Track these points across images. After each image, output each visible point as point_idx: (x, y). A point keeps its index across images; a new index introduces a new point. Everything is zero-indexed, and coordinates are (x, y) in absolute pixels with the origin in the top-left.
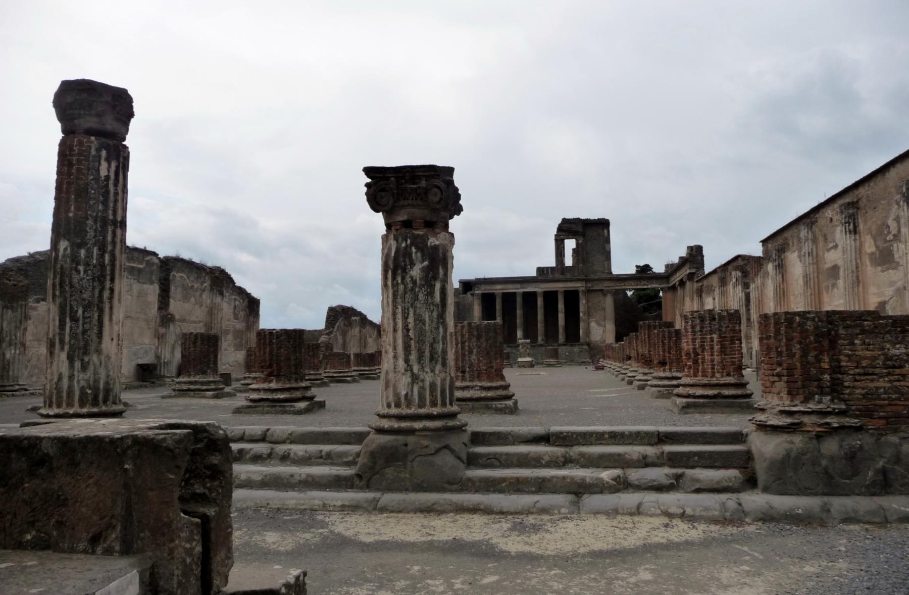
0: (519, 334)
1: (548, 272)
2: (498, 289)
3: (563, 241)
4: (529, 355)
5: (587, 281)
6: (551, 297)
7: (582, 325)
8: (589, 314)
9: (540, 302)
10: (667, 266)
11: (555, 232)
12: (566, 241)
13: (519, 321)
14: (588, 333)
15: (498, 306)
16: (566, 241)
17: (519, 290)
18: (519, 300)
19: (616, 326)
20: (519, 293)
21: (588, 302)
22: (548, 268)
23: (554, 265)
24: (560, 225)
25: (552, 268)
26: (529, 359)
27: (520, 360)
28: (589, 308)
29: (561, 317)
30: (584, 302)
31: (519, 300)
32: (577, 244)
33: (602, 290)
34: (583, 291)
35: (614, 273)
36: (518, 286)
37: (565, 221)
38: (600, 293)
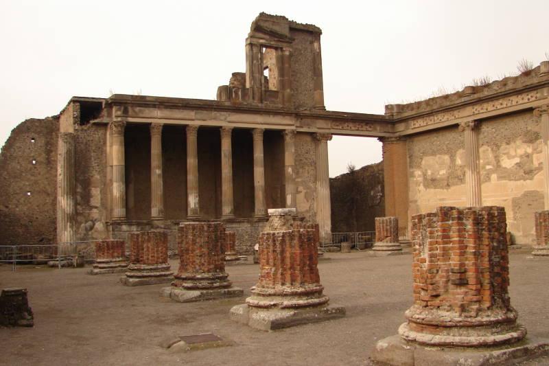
0: (193, 201)
2: (158, 118)
5: (298, 116)
6: (242, 138)
9: (226, 145)
10: (387, 107)
11: (247, 30)
13: (192, 177)
17: (194, 121)
18: (192, 140)
29: (259, 172)
31: (192, 140)
33: (312, 134)
34: (293, 132)
36: (192, 114)
37: (263, 15)
38: (308, 139)
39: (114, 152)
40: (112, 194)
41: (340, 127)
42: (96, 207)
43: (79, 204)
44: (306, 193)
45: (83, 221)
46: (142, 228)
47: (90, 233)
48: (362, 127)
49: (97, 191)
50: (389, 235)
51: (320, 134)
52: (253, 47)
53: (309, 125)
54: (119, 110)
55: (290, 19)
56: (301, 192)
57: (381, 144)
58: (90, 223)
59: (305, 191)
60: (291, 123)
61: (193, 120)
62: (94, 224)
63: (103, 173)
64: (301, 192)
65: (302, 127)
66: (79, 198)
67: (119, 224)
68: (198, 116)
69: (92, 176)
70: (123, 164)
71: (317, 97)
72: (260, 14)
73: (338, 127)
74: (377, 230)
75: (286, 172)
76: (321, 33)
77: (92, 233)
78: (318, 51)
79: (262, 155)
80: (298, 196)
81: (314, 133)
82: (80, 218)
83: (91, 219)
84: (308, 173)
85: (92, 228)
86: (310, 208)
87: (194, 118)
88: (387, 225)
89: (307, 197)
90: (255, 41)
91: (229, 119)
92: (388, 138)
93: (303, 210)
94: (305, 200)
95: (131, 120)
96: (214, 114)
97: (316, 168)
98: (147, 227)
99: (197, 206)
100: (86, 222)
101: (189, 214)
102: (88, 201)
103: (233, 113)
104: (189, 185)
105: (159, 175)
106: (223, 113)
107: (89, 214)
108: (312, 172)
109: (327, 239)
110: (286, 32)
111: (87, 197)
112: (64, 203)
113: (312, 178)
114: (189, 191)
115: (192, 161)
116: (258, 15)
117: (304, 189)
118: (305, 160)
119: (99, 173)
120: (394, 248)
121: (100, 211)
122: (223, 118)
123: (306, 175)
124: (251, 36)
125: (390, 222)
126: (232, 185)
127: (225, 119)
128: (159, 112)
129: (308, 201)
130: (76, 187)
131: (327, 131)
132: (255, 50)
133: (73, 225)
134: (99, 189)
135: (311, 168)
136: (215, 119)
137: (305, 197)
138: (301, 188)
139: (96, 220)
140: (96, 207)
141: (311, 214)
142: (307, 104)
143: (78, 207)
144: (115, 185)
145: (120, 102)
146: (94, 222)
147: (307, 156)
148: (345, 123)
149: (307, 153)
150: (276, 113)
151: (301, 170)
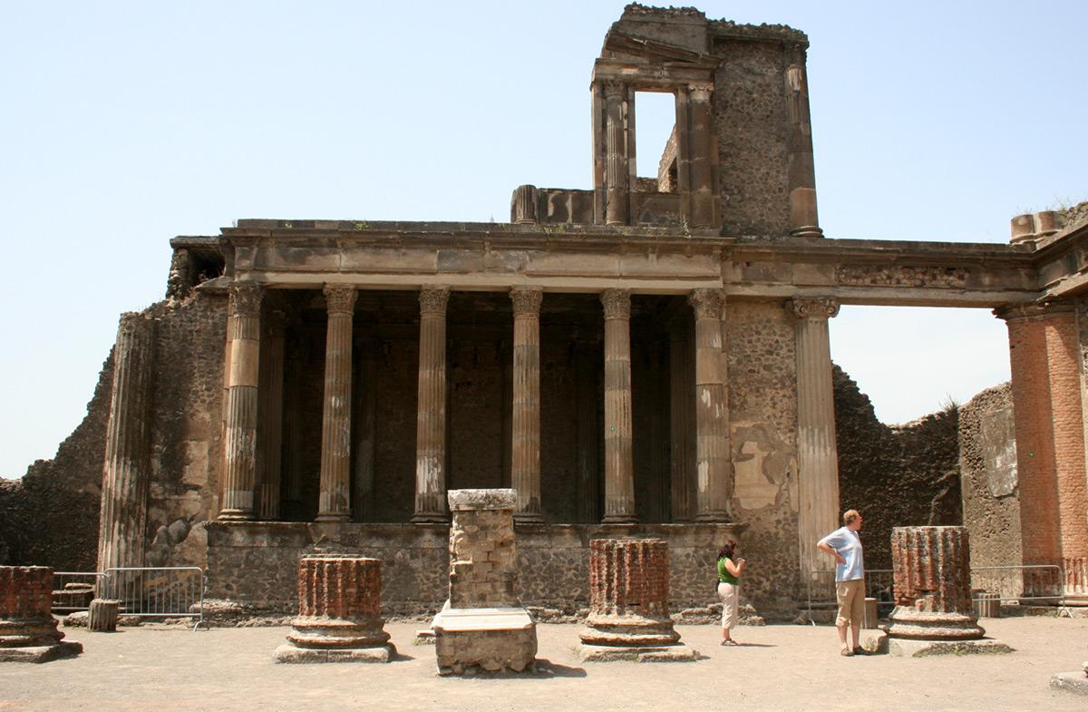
1: (560, 214)
2: (341, 272)
3: (629, 88)
4: (513, 594)
6: (571, 322)
7: (707, 445)
8: (733, 402)
9: (525, 334)
12: (641, 97)
13: (429, 416)
14: (727, 479)
15: (337, 345)
16: (641, 97)
17: (437, 276)
18: (432, 320)
19: (839, 454)
20: (436, 292)
21: (727, 348)
22: (564, 192)
23: (587, 183)
24: (616, 28)
25: (579, 195)
26: (516, 619)
27: (451, 618)
28: (731, 373)
30: (717, 344)
31: (432, 320)
32: (686, 116)
33: (785, 303)
34: (712, 294)
35: (827, 234)
36: (432, 259)
38: (775, 315)
39: (237, 359)
40: (223, 460)
41: (868, 281)
42: (196, 488)
43: (157, 480)
44: (766, 459)
45: (163, 519)
46: (282, 541)
47: (178, 548)
48: (934, 277)
49: (201, 449)
50: (929, 585)
51: (803, 299)
52: (613, 98)
53: (769, 279)
54: (245, 256)
55: (712, 15)
56: (751, 456)
57: (1003, 322)
58: (178, 525)
59: (766, 454)
60: (709, 272)
61: (433, 274)
62: (189, 528)
63: (215, 405)
64: (751, 456)
65: (749, 284)
66: (156, 464)
67: (224, 528)
68: (446, 265)
69: (192, 415)
70: (254, 382)
71: (796, 204)
72: (629, 9)
73: (860, 281)
74: (897, 567)
75: (698, 400)
76: (807, 45)
77: (183, 549)
78: (797, 88)
79: (627, 358)
80: (741, 467)
81: (790, 299)
82: (155, 513)
83: (182, 515)
84: (774, 407)
85: (182, 537)
86: (777, 499)
87: (435, 267)
88: (920, 553)
89: (768, 471)
90: (609, 71)
91: (530, 267)
92: (1018, 306)
93: (758, 505)
94: (766, 481)
95: (272, 278)
96: (489, 255)
97: (794, 390)
98: (297, 538)
99: (435, 489)
100: (171, 520)
101: (418, 507)
102: (181, 473)
103: (544, 253)
104: (420, 437)
105: (338, 412)
106: (513, 253)
107: (178, 502)
108: (784, 404)
109: (823, 586)
110: (699, 45)
111: (176, 462)
112: (115, 477)
113: (784, 420)
114: (419, 452)
115: (430, 376)
116: (623, 11)
117: (762, 449)
118: (762, 371)
119: (210, 408)
120: (948, 631)
121: (205, 498)
122: (514, 265)
123: (768, 411)
124: (598, 62)
125: (933, 542)
126: (537, 438)
127: (520, 269)
128: (344, 257)
129: (772, 481)
130: (150, 438)
131: (826, 291)
132: (612, 94)
133: (128, 525)
134: (205, 445)
135: (781, 393)
136: (494, 269)
137: (764, 471)
138: (750, 447)
139: (192, 519)
140: (196, 488)
141: (781, 516)
142: (769, 225)
143: (154, 485)
144: (228, 429)
145: (248, 236)
146: (188, 521)
147: (770, 360)
148: (879, 269)
149: (771, 353)
150: (667, 248)
151: (751, 399)
